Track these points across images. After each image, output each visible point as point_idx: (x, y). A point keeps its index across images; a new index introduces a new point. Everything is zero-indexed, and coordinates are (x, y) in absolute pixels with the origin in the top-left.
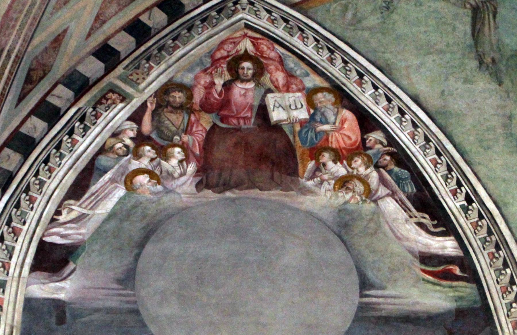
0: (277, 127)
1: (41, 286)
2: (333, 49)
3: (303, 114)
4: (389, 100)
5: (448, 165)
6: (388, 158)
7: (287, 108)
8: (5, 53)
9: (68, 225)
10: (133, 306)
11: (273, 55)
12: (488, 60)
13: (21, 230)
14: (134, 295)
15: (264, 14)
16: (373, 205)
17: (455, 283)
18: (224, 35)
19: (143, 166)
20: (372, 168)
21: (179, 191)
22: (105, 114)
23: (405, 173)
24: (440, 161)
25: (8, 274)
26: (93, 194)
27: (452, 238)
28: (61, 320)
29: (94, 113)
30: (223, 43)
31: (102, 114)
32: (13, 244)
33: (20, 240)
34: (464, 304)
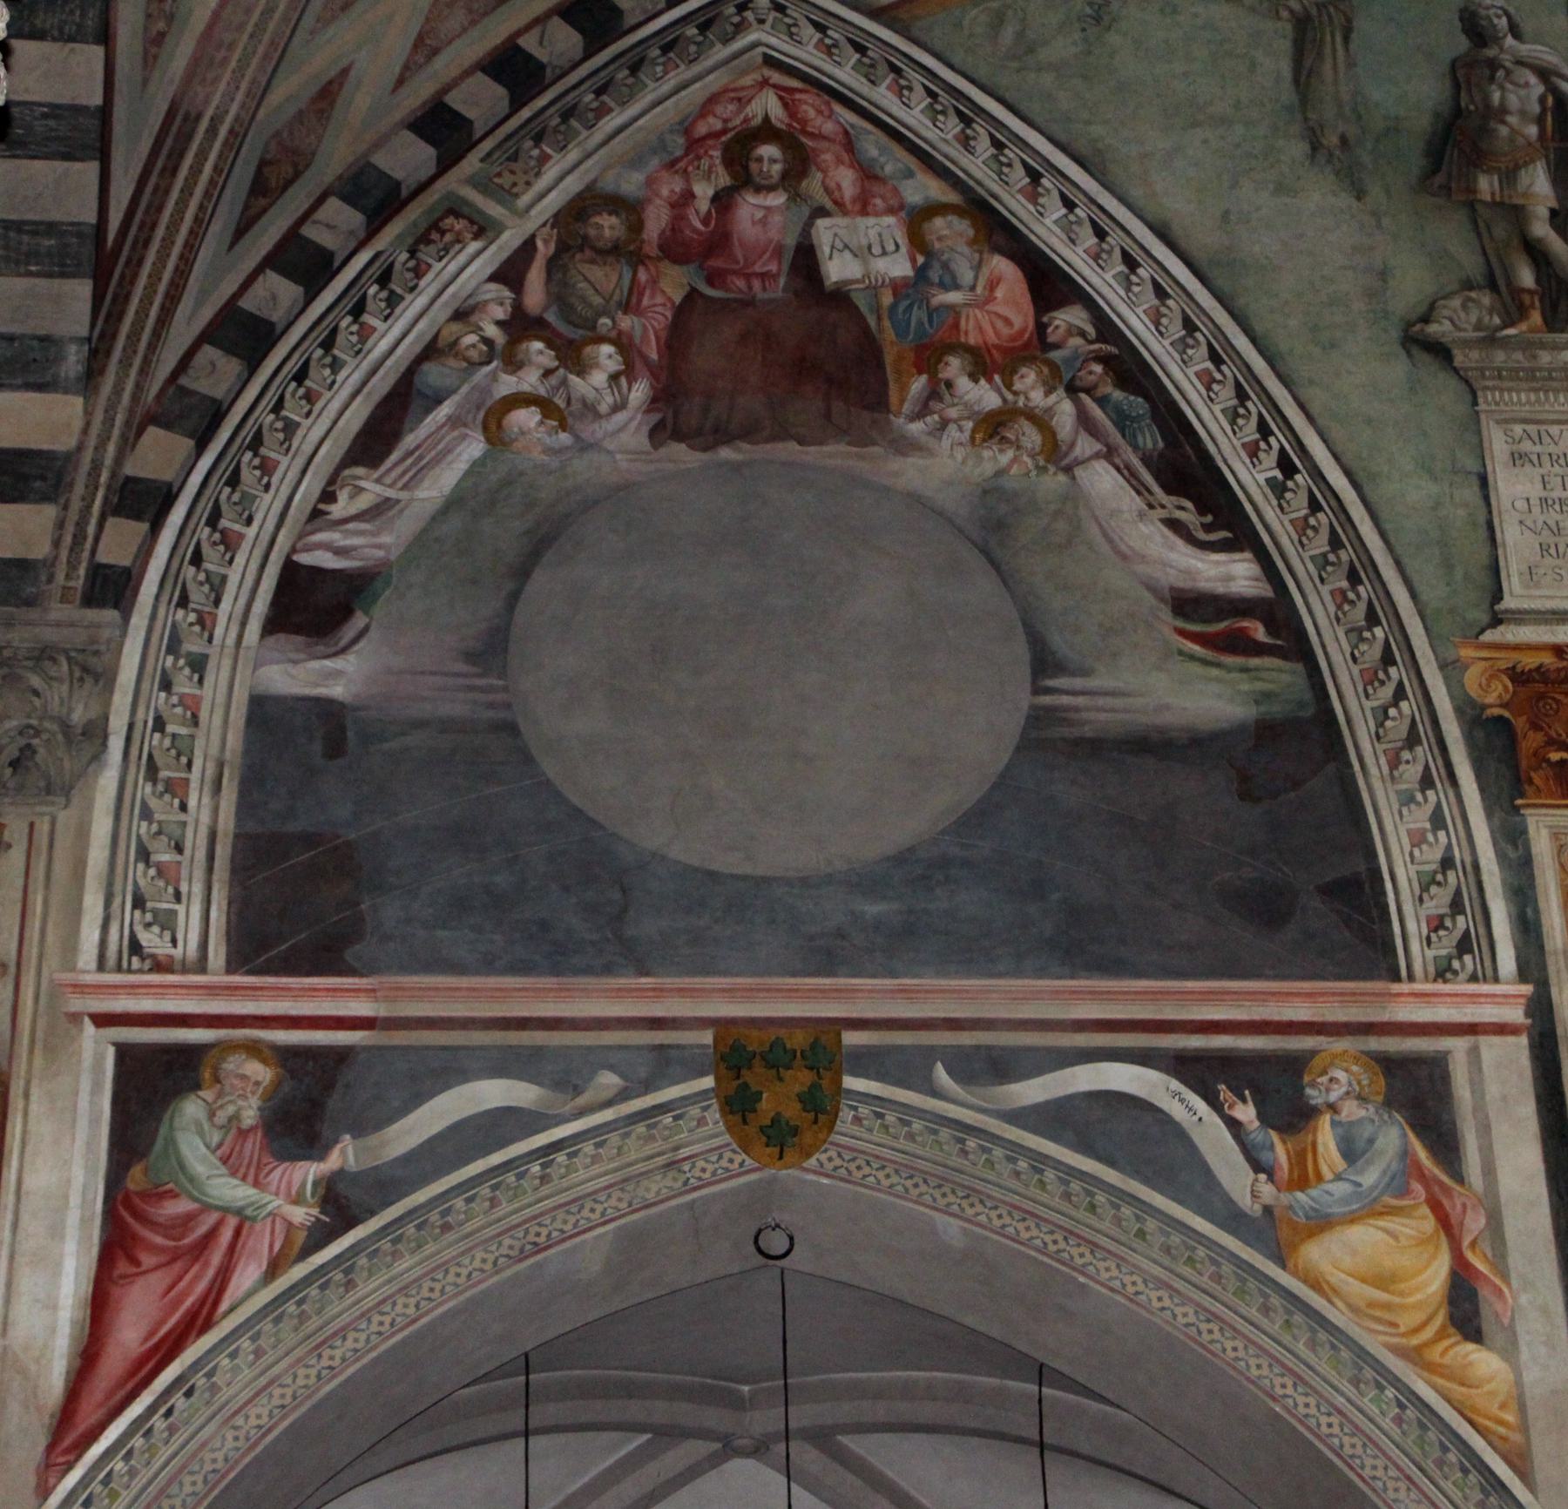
0: (840, 297)
1: (289, 667)
2: (968, 115)
3: (899, 267)
4: (1101, 234)
5: (1238, 386)
6: (1098, 368)
7: (863, 253)
8: (204, 124)
9: (351, 526)
10: (502, 715)
11: (829, 127)
12: (1332, 140)
13: (241, 536)
14: (505, 689)
15: (808, 32)
16: (1062, 478)
17: (1255, 662)
18: (714, 82)
19: (526, 388)
20: (1061, 392)
21: (610, 445)
22: (438, 266)
23: (1137, 405)
24: (1218, 376)
25: (210, 640)
26: (409, 454)
27: (1248, 555)
28: (335, 747)
29: (412, 264)
30: (713, 99)
31: (429, 266)
32: (222, 571)
33: (240, 559)
34: (1276, 710)
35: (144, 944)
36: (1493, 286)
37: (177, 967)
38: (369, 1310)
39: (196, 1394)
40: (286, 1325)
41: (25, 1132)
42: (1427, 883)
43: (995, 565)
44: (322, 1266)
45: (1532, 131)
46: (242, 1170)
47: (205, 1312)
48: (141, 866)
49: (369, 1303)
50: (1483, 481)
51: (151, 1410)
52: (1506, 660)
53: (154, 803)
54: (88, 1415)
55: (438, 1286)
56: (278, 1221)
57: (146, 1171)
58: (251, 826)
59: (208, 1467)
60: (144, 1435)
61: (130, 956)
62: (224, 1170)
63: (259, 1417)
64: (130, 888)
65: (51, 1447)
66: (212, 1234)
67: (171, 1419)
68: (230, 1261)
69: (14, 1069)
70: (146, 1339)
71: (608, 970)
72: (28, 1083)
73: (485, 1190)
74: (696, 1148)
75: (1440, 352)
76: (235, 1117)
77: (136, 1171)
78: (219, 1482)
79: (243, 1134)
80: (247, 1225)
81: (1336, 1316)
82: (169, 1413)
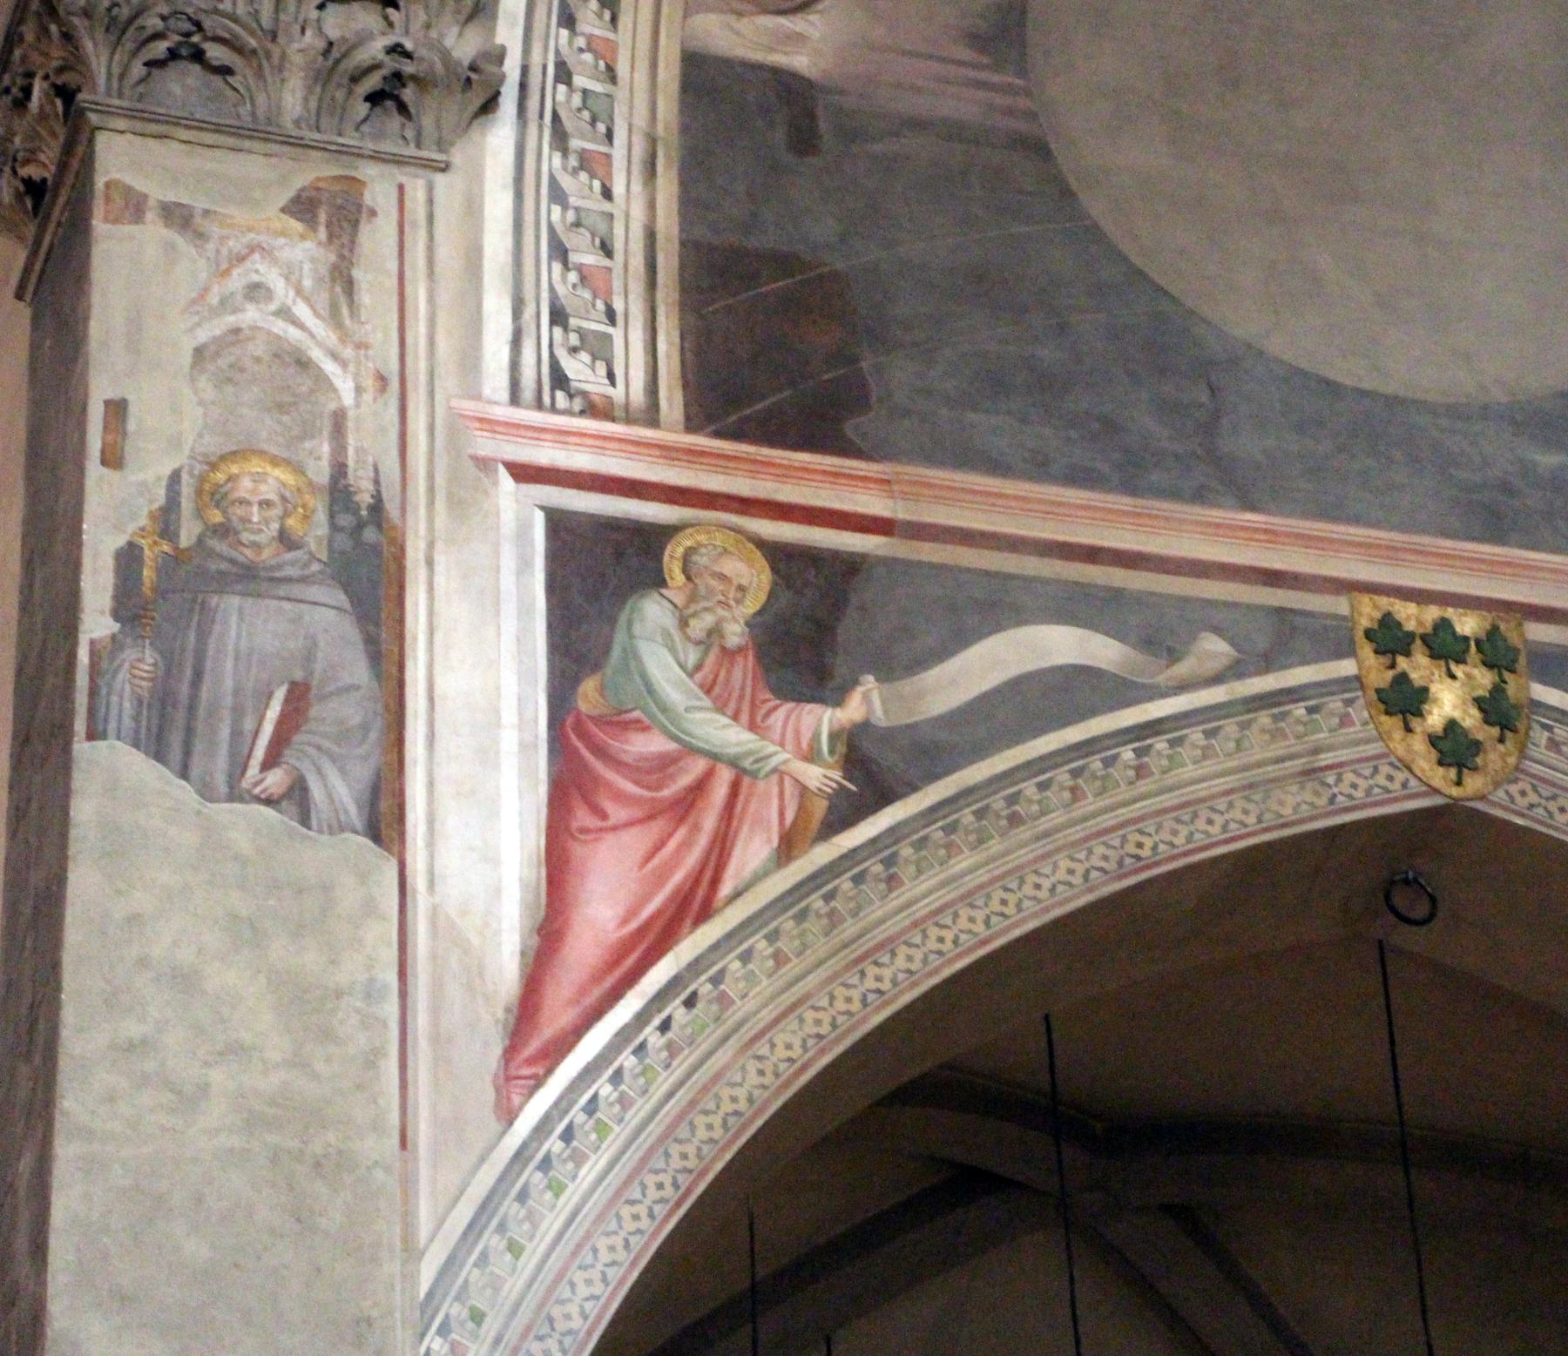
1: (732, 19)
10: (1021, 126)
14: (1028, 93)
28: (804, 140)
35: (570, 375)
37: (619, 413)
38: (924, 920)
39: (700, 1005)
40: (813, 926)
41: (431, 613)
44: (854, 851)
46: (732, 705)
47: (701, 893)
48: (557, 267)
49: (921, 910)
51: (641, 1019)
53: (566, 181)
54: (556, 1015)
55: (1012, 899)
56: (788, 782)
57: (602, 689)
58: (700, 232)
59: (728, 1107)
60: (635, 1052)
61: (553, 389)
62: (707, 702)
63: (789, 1047)
64: (545, 295)
65: (510, 1052)
66: (700, 787)
67: (670, 1035)
68: (728, 825)
69: (410, 522)
70: (625, 921)
71: (1199, 496)
72: (431, 545)
73: (1062, 776)
74: (1343, 755)
76: (715, 632)
77: (589, 686)
78: (744, 1127)
79: (729, 654)
80: (746, 781)
82: (665, 1027)
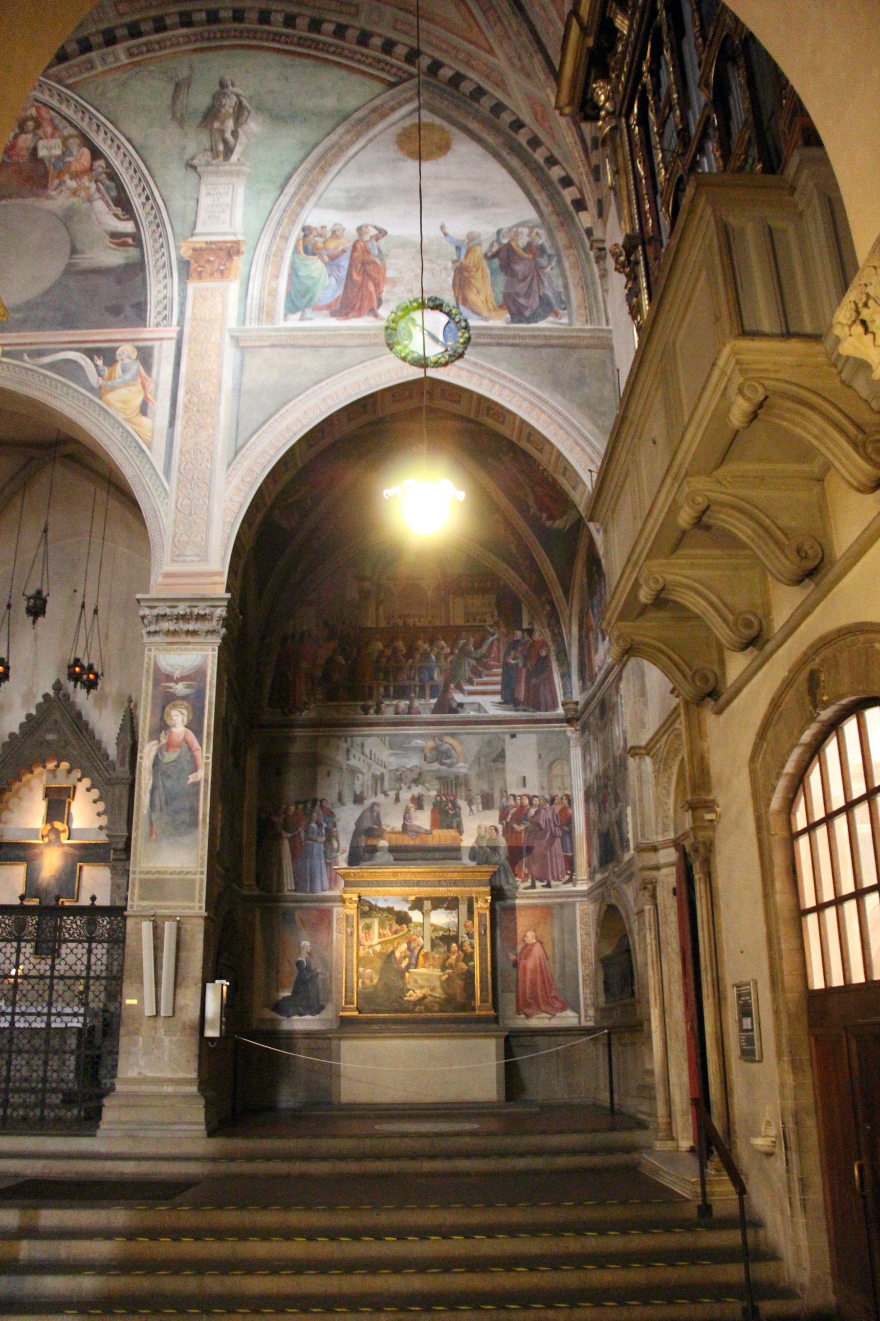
0: (41, 161)
7: (49, 149)
12: (178, 115)
23: (112, 184)
34: (130, 261)
36: (212, 150)
42: (159, 303)
43: (67, 228)
45: (231, 110)
50: (198, 200)
52: (192, 246)
75: (194, 168)
81: (112, 412)
